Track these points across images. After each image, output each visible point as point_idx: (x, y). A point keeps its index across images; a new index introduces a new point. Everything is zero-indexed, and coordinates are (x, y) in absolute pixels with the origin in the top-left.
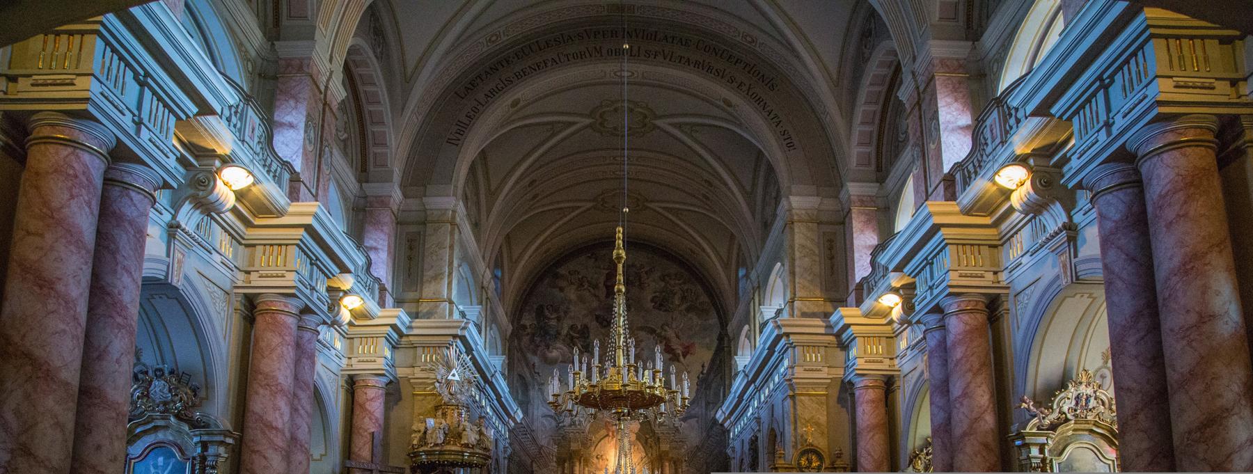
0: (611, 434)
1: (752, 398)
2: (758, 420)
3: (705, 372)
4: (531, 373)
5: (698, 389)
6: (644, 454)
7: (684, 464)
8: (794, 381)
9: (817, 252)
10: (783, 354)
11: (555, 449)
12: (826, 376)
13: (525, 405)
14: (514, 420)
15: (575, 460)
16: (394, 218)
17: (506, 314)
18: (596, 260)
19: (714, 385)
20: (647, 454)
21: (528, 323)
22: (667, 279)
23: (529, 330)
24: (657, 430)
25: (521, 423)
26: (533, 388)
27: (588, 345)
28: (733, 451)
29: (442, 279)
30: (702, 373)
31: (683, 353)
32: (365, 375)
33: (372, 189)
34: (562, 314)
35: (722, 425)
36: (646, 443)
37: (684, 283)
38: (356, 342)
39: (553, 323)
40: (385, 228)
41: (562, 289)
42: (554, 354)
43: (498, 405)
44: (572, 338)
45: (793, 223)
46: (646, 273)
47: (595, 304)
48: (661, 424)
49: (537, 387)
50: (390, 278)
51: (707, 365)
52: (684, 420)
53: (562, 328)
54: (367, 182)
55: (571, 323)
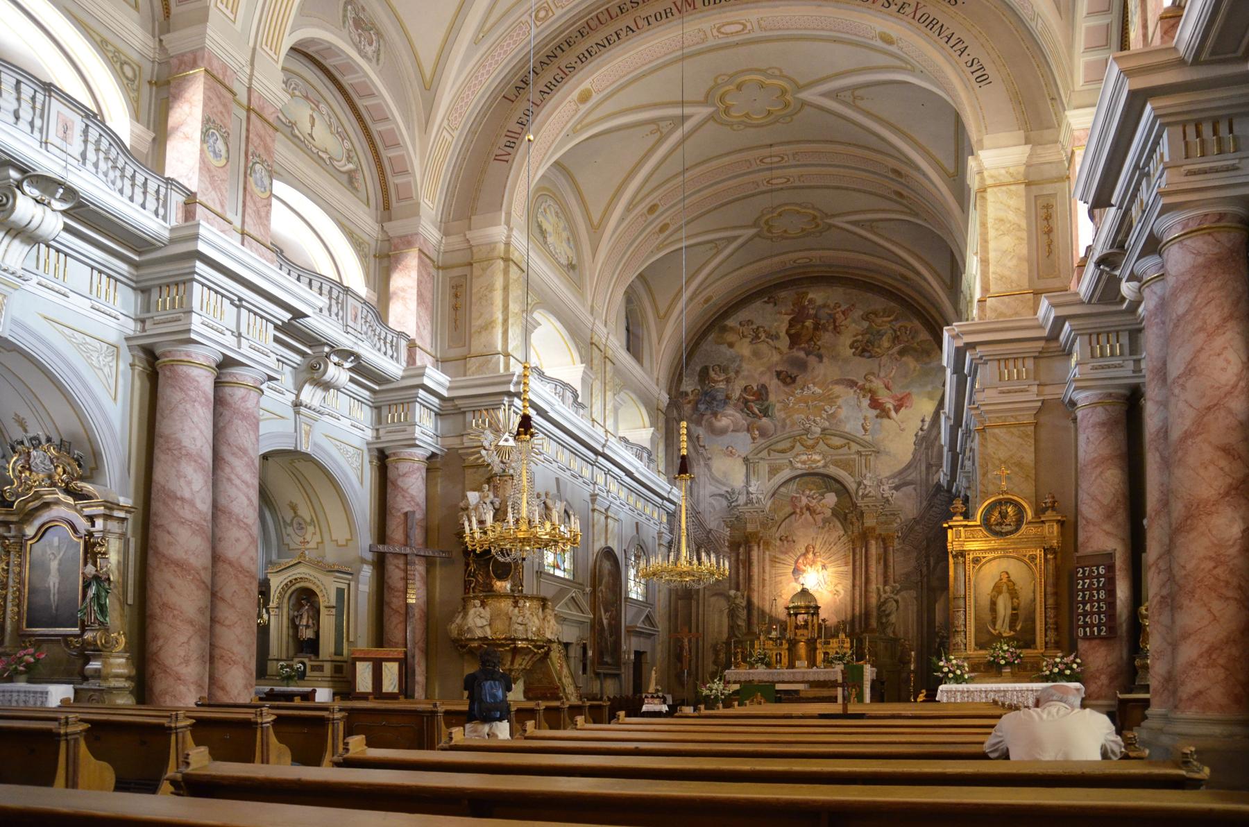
0: (798, 511)
22: (872, 316)
27: (767, 408)
32: (395, 447)
34: (732, 374)
39: (722, 385)
41: (731, 345)
44: (746, 402)
48: (864, 496)
52: (897, 488)
53: (733, 390)
55: (743, 383)
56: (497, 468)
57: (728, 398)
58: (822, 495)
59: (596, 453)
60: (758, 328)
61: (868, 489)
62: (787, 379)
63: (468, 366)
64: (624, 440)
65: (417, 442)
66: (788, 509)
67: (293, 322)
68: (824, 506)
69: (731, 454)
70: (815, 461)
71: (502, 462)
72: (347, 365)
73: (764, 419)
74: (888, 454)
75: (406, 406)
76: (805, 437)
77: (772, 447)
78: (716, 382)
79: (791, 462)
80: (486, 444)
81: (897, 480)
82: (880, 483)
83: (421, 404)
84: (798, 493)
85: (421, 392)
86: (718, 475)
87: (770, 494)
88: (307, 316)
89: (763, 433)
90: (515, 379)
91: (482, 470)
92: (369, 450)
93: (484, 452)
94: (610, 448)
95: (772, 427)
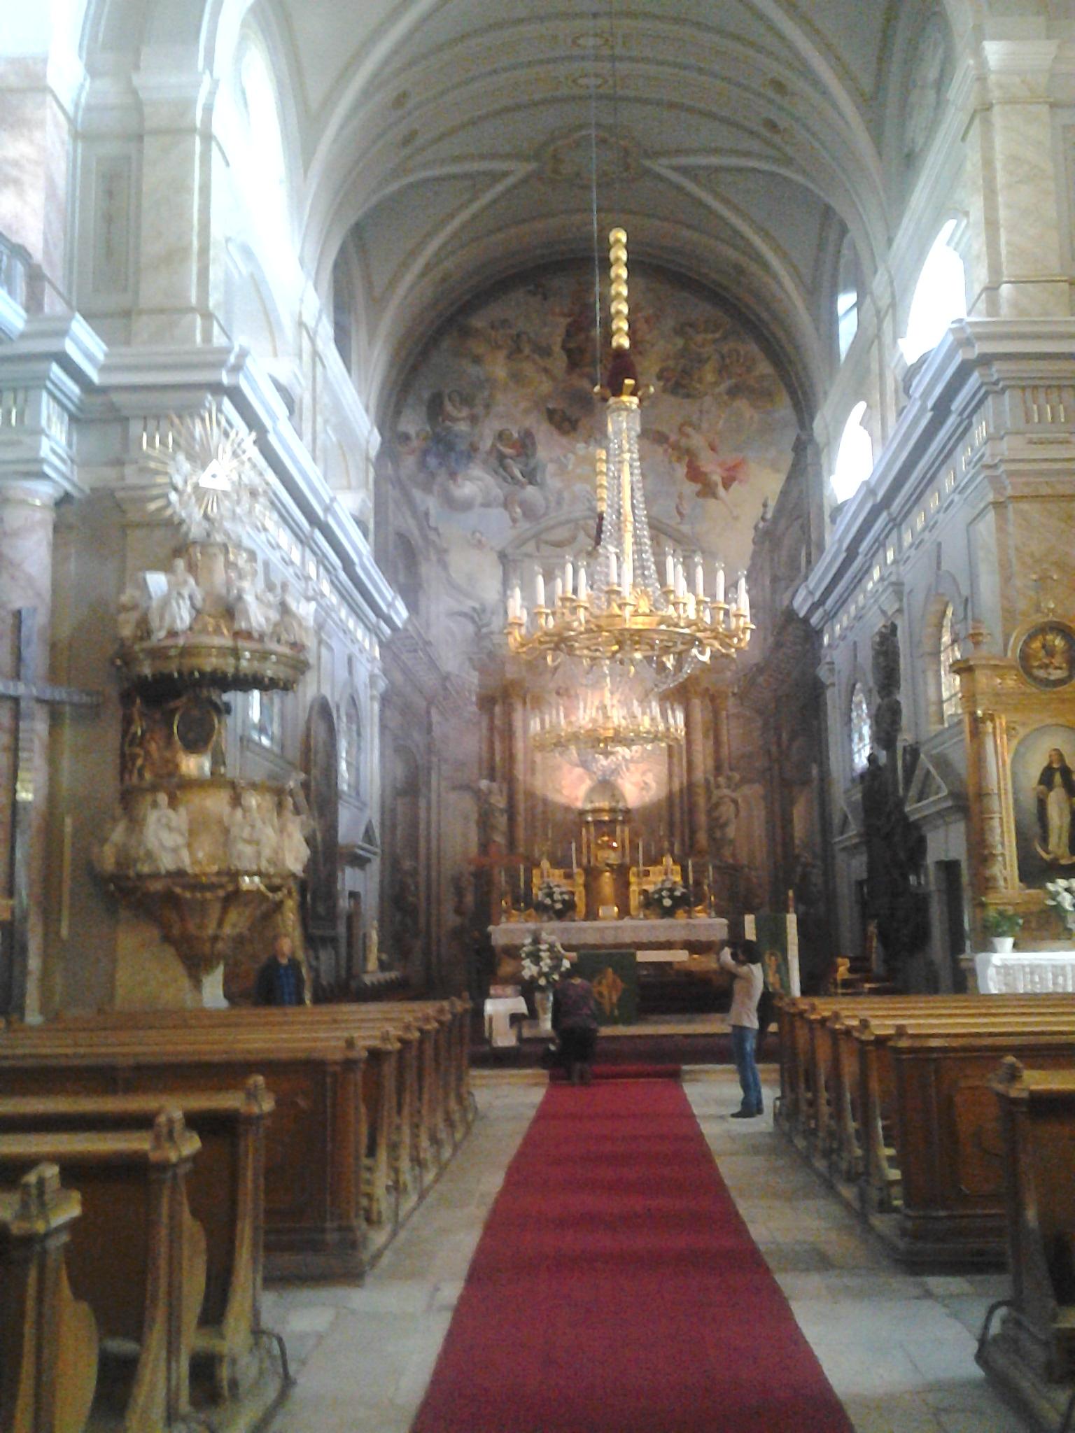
1: (880, 544)
2: (898, 588)
3: (769, 516)
4: (421, 529)
10: (970, 416)
13: (411, 592)
14: (389, 621)
17: (367, 410)
18: (545, 298)
19: (787, 542)
21: (412, 430)
23: (415, 443)
25: (406, 630)
26: (428, 559)
27: (534, 469)
28: (832, 670)
30: (763, 519)
31: (723, 478)
35: (806, 620)
37: (725, 338)
41: (477, 360)
44: (502, 457)
46: (647, 321)
47: (546, 387)
49: (434, 557)
51: (772, 504)
56: (196, 529)
57: (474, 448)
60: (518, 336)
65: (47, 469)
69: (479, 545)
71: (206, 516)
73: (530, 489)
75: (21, 396)
77: (545, 536)
78: (455, 420)
80: (178, 480)
83: (51, 393)
89: (529, 512)
90: (232, 359)
91: (159, 534)
95: (542, 502)
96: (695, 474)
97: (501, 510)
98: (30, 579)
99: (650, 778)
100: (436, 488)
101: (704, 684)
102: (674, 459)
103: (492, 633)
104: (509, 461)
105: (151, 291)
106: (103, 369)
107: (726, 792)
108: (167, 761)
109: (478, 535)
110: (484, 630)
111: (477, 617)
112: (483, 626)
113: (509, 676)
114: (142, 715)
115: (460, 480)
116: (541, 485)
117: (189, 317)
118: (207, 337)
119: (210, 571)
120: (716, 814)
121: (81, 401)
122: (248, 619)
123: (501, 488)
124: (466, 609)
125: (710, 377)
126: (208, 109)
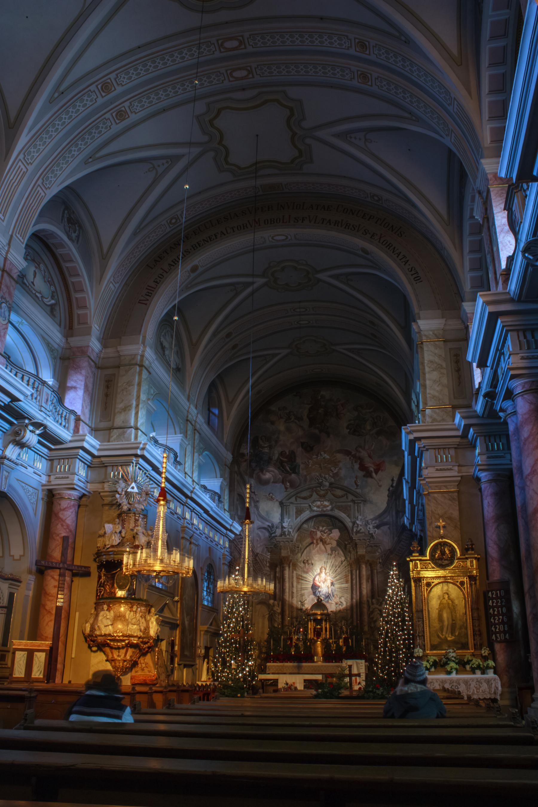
0: (315, 541)
3: (394, 485)
5: (388, 500)
6: (343, 558)
7: (379, 565)
8: (427, 480)
9: (444, 365)
11: (268, 555)
12: (456, 474)
15: (285, 565)
16: (92, 364)
20: (346, 558)
24: (355, 537)
29: (130, 410)
30: (392, 486)
31: (374, 469)
32: (61, 489)
33: (76, 341)
35: (411, 530)
36: (345, 548)
38: (56, 462)
39: (266, 450)
40: (83, 372)
41: (273, 423)
42: (267, 476)
43: (209, 519)
44: (282, 462)
45: (422, 343)
48: (358, 532)
50: (87, 411)
51: (396, 479)
52: (378, 527)
54: (72, 336)
57: (270, 459)
58: (330, 530)
59: (186, 496)
61: (360, 527)
62: (308, 448)
63: (112, 435)
64: (204, 488)
65: (75, 487)
66: (309, 540)
67: (11, 404)
68: (331, 538)
69: (272, 499)
70: (326, 506)
72: (38, 432)
73: (293, 475)
74: (371, 502)
76: (319, 489)
77: (299, 495)
79: (310, 506)
80: (119, 490)
81: (377, 521)
82: (367, 524)
84: (315, 529)
85: (81, 452)
86: (263, 514)
87: (296, 529)
88: (21, 401)
89: (293, 485)
90: (141, 446)
92: (43, 490)
93: (117, 496)
94: (196, 494)
96: (363, 467)
97: (281, 484)
98: (68, 526)
99: (343, 600)
100: (254, 476)
101: (367, 558)
102: (354, 461)
103: (276, 536)
104: (286, 464)
105: (118, 421)
106: (99, 450)
107: (377, 606)
108: (112, 593)
109: (271, 495)
110: (273, 535)
111: (270, 529)
112: (272, 533)
113: (283, 555)
114: (105, 575)
115: (264, 472)
116: (297, 473)
117: (130, 429)
118: (136, 437)
119: (129, 523)
120: (371, 616)
121: (91, 461)
122: (139, 542)
123: (281, 475)
124: (266, 526)
125: (368, 427)
126: (142, 356)
